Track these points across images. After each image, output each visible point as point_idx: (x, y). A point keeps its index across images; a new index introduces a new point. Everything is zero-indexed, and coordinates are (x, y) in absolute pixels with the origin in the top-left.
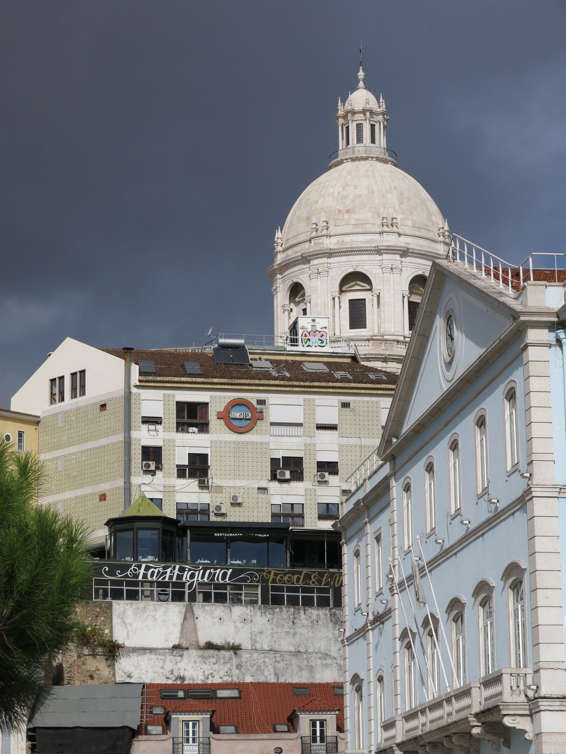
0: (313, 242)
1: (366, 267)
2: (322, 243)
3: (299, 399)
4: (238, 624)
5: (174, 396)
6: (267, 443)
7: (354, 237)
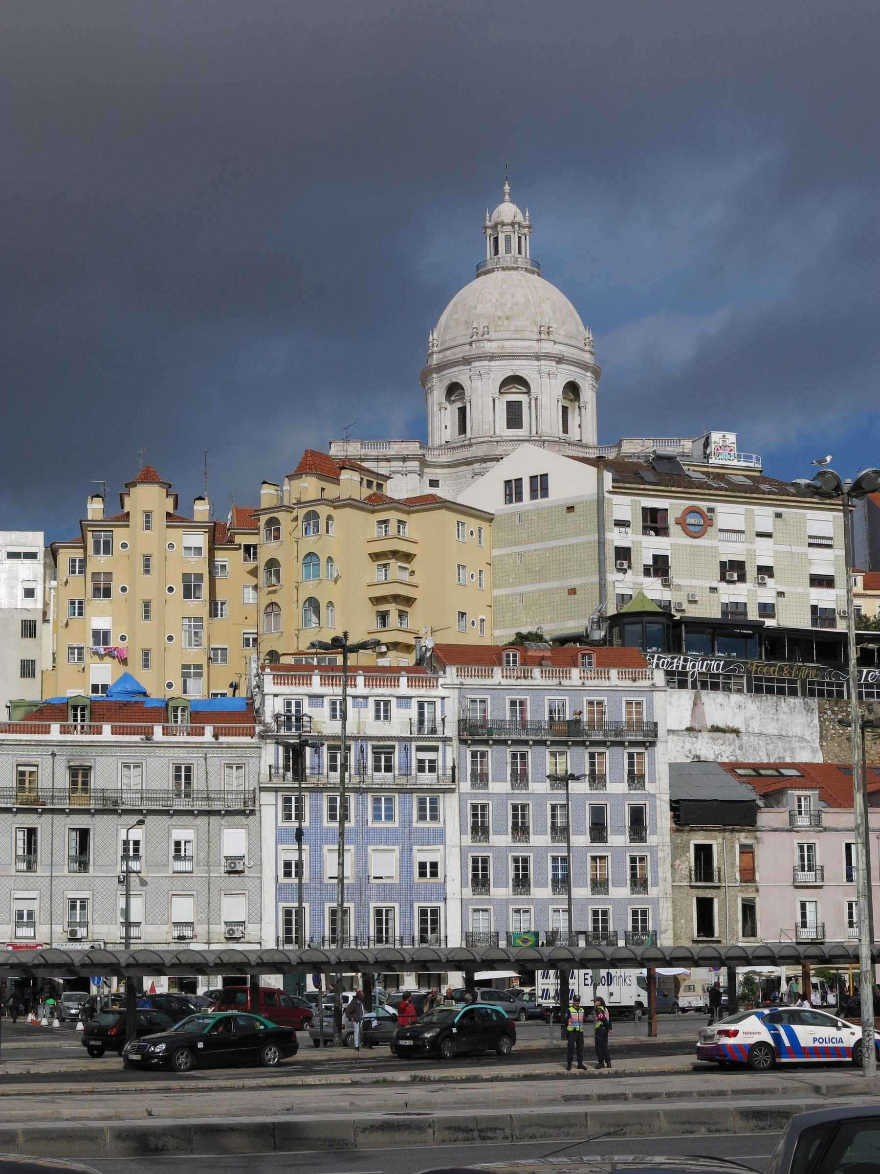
0: (474, 345)
1: (525, 372)
3: (741, 508)
4: (734, 710)
5: (640, 502)
6: (717, 548)
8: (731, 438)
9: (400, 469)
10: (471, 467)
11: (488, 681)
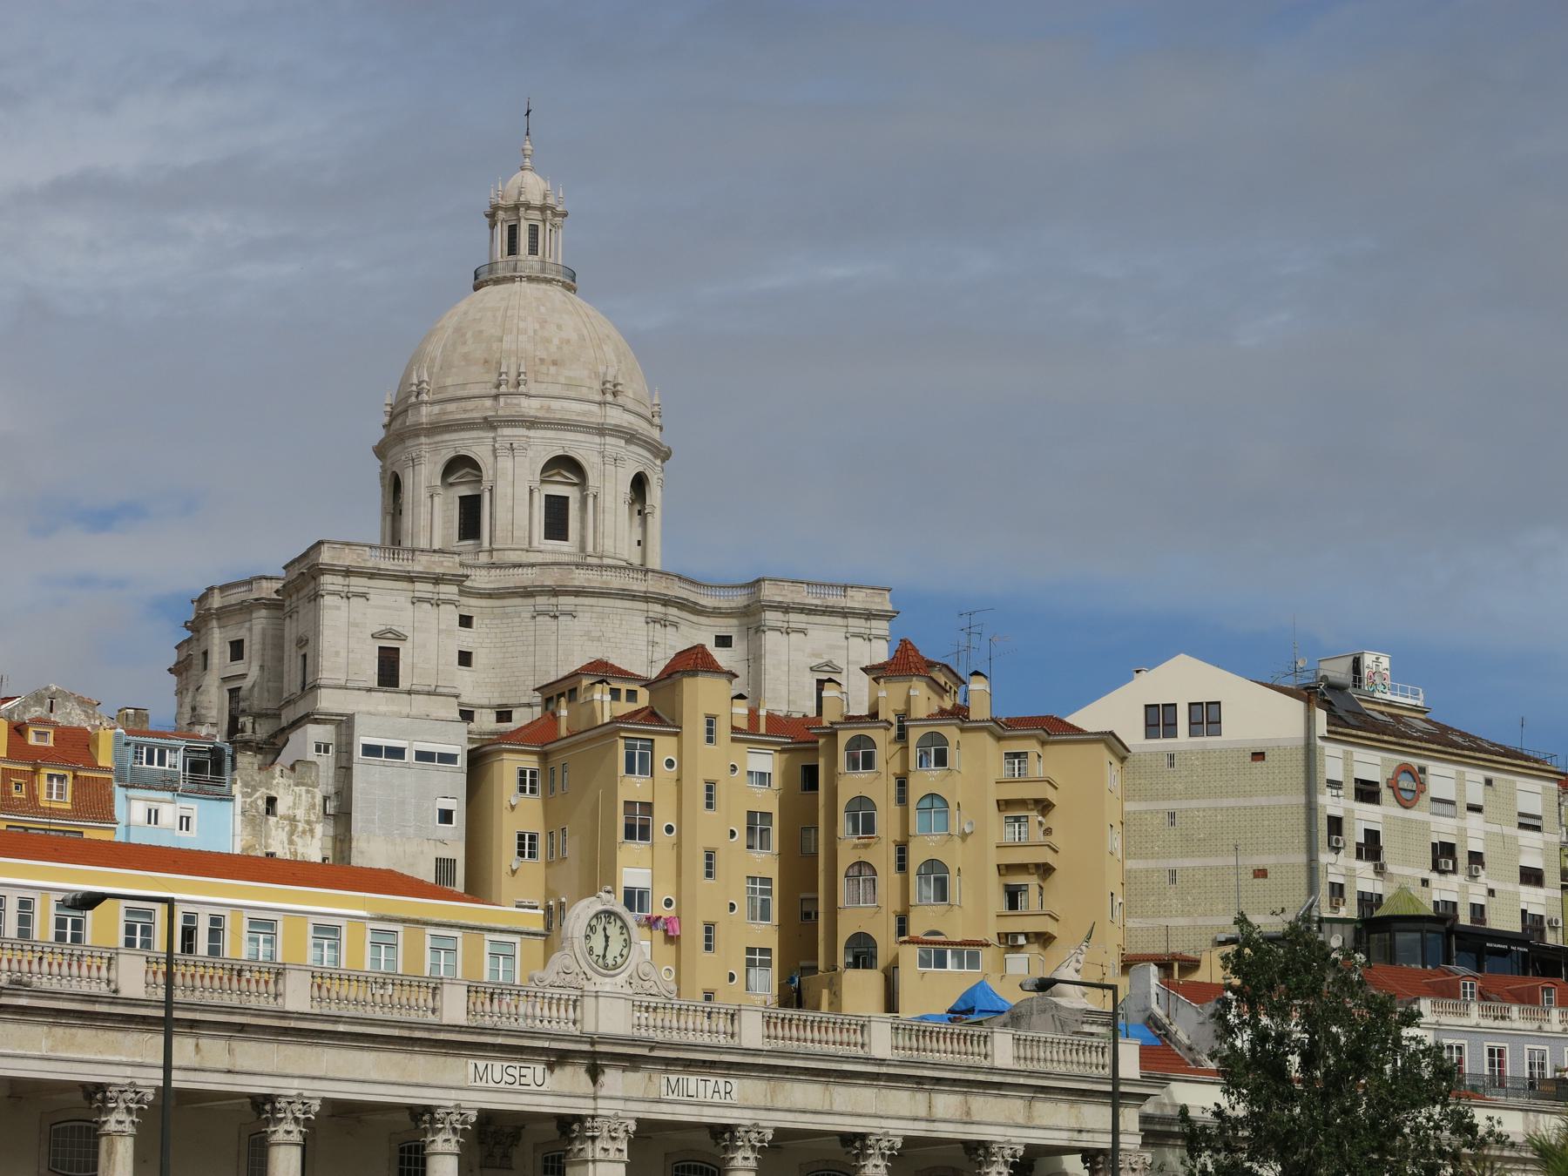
0: (502, 400)
6: (1428, 823)
8: (1385, 662)
10: (531, 601)
11: (1464, 1021)
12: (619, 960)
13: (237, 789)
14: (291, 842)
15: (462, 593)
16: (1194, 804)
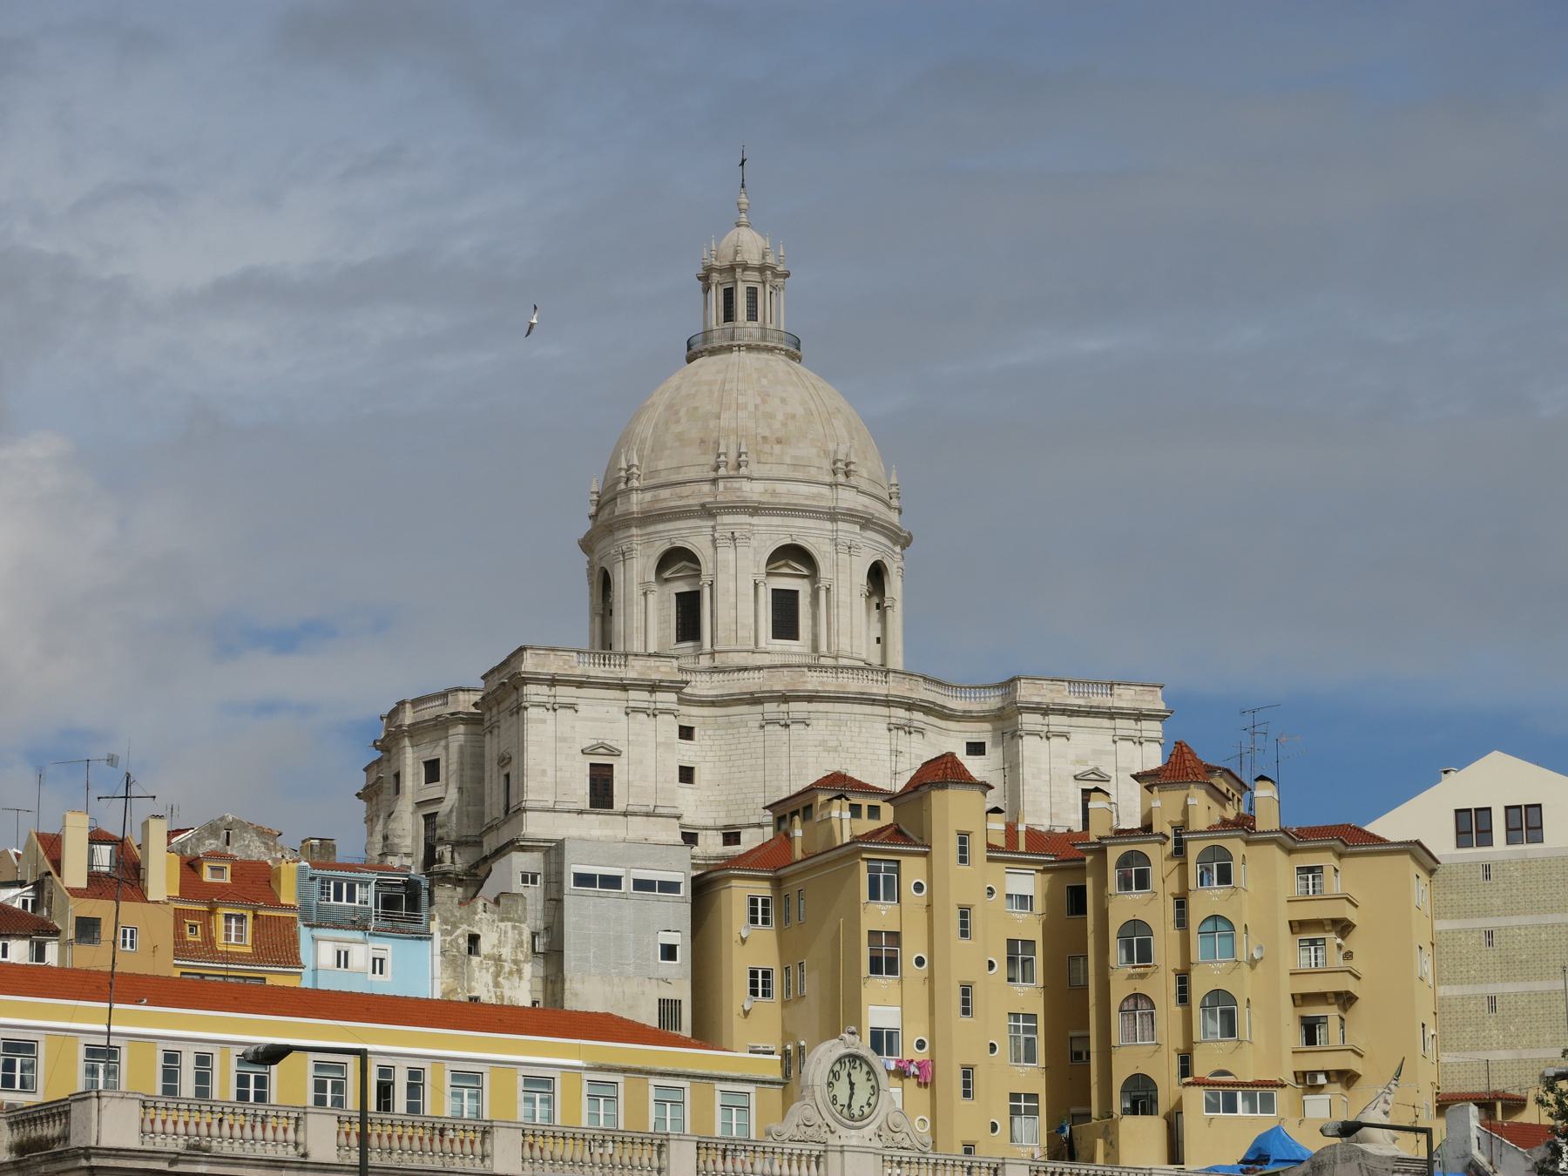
0: (721, 484)
2: (740, 489)
7: (793, 487)
9: (645, 705)
10: (759, 708)
12: (866, 1110)
13: (435, 927)
14: (497, 985)
15: (681, 701)
16: (1515, 921)
